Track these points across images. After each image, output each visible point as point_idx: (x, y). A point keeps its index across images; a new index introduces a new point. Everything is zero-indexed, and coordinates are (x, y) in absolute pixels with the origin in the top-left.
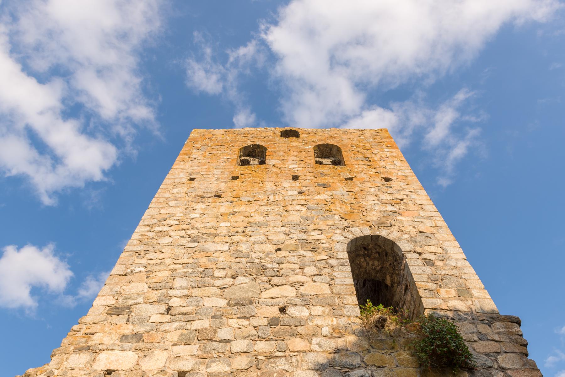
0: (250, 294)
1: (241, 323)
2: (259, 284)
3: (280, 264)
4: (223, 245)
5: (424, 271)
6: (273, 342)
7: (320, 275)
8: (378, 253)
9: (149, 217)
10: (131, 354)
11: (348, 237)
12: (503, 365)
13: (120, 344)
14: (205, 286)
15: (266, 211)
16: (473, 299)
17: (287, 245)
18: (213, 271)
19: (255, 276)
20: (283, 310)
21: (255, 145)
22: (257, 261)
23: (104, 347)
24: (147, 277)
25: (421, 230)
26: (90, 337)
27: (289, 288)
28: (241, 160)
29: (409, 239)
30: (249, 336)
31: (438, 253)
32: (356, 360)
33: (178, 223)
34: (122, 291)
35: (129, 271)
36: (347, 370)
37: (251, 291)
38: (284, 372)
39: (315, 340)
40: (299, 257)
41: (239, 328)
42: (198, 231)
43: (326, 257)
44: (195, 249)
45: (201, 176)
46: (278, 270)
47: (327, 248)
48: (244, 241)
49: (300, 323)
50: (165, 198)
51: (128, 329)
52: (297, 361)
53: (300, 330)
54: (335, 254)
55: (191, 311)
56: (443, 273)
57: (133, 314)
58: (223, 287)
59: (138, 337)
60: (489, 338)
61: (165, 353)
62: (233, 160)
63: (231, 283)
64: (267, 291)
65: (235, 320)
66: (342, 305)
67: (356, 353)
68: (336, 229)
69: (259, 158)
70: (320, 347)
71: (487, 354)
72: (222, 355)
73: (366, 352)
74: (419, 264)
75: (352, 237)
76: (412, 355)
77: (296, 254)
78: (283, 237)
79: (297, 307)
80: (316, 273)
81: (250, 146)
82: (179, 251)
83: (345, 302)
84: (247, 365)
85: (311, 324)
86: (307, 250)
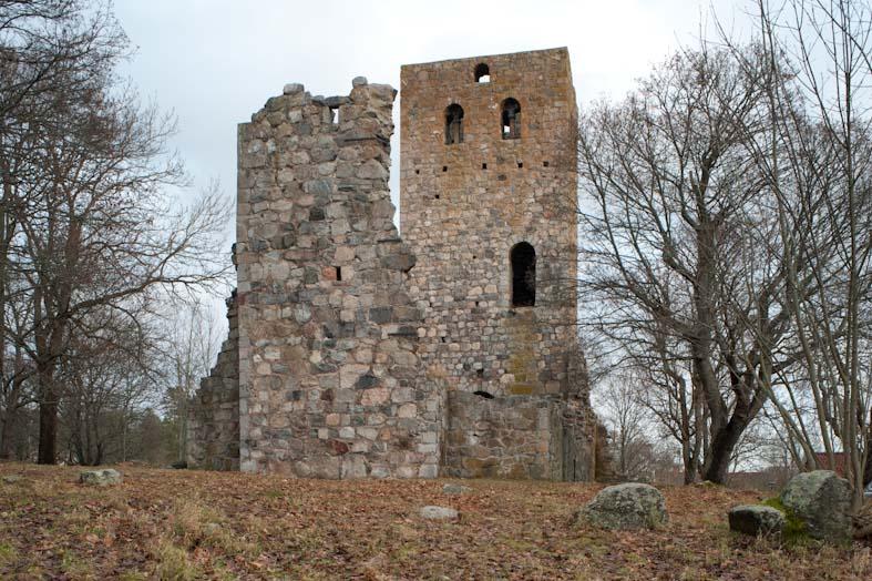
20: (477, 303)
32: (502, 331)
49: (484, 311)
53: (484, 315)
75: (512, 244)
78: (476, 245)
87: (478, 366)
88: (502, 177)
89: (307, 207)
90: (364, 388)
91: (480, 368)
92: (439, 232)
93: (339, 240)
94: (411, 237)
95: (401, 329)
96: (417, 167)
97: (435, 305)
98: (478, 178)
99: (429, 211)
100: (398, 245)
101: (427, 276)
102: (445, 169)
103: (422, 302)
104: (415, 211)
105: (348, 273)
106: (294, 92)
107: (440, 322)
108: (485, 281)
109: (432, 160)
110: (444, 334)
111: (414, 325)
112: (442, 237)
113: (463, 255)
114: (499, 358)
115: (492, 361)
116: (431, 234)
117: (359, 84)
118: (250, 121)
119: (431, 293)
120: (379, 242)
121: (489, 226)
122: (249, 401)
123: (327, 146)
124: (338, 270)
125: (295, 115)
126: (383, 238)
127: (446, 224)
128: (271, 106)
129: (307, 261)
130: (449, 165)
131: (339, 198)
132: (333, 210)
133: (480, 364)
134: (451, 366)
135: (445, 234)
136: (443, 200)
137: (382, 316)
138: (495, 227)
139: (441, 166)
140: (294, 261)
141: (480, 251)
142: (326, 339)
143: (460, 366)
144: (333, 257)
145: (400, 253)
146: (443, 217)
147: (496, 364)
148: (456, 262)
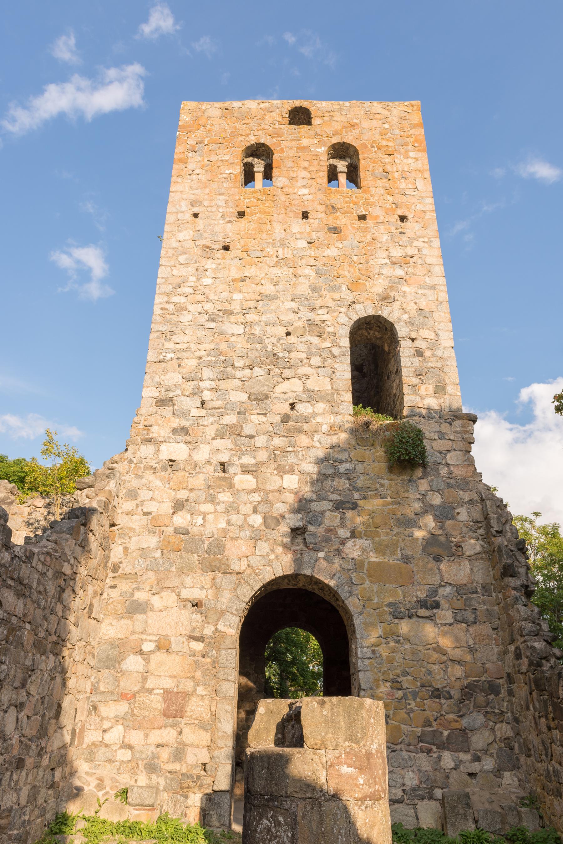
0: (266, 388)
1: (260, 420)
2: (273, 377)
3: (289, 352)
4: (238, 326)
5: (412, 364)
6: (285, 439)
7: (324, 367)
8: (379, 327)
9: (164, 280)
10: (182, 445)
11: (351, 317)
12: (449, 462)
13: (173, 437)
14: (228, 378)
15: (276, 275)
16: (445, 397)
17: (296, 328)
18: (233, 361)
19: (269, 367)
20: (292, 406)
21: (259, 143)
22: (270, 348)
23: (163, 440)
24: (179, 366)
25: (421, 308)
26: (149, 429)
27: (296, 380)
28: (244, 164)
29: (408, 320)
30: (267, 432)
31: (431, 340)
32: (345, 456)
33: (193, 292)
34: (162, 382)
35: (162, 357)
36: (338, 464)
37: (267, 385)
38: (293, 464)
39: (317, 437)
40: (306, 343)
41: (259, 424)
42: (213, 305)
43: (330, 345)
44: (214, 331)
45: (205, 208)
46: (288, 360)
47: (332, 333)
48: (257, 321)
49: (306, 420)
50: (173, 248)
51: (176, 423)
52: (303, 455)
53: (306, 427)
54: (338, 341)
55: (221, 406)
56: (429, 365)
57: (176, 407)
58: (243, 379)
59: (184, 431)
60: (446, 437)
61: (207, 446)
62: (236, 176)
63: (249, 375)
64: (280, 385)
65: (256, 416)
66: (339, 402)
67: (345, 450)
68: (341, 307)
69: (264, 158)
70: (320, 443)
71: (440, 453)
72: (249, 449)
73: (352, 449)
74: (411, 354)
75: (355, 318)
76: (385, 452)
77: (304, 340)
78: (292, 316)
79: (303, 403)
80: (320, 364)
81: (254, 144)
82: (201, 333)
83: (342, 399)
84: (267, 458)
85: (314, 421)
86: (313, 335)
88: (335, 230)
94: (176, 299)
96: (196, 210)
97: (208, 405)
99: (210, 265)
104: (186, 264)
107: (220, 435)
108: (306, 370)
110: (224, 457)
112: (230, 301)
113: (268, 328)
114: (339, 506)
115: (323, 512)
116: (212, 297)
119: (202, 385)
134: (237, 519)
135: (237, 296)
136: (235, 252)
138: (324, 293)
139: (235, 211)
141: (300, 324)
143: (257, 520)
146: (235, 273)
148: (253, 339)
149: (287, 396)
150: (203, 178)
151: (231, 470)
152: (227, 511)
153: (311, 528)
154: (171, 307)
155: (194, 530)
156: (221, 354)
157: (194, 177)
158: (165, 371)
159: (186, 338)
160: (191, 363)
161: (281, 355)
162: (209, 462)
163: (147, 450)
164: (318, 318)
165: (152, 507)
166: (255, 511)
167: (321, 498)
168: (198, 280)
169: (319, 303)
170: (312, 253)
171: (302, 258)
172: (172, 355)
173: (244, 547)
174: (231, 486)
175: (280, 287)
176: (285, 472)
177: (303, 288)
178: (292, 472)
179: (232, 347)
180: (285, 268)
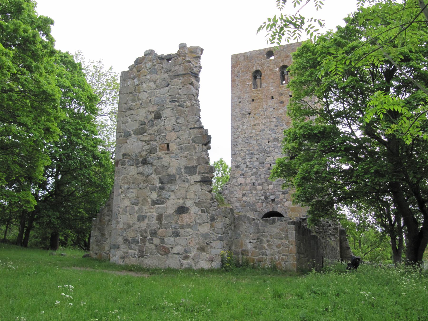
20: (271, 165)
51: (241, 172)
59: (243, 175)
78: (269, 136)
87: (272, 197)
88: (282, 102)
89: (153, 112)
90: (180, 214)
91: (273, 198)
92: (250, 131)
93: (169, 128)
94: (237, 134)
95: (202, 178)
96: (240, 100)
98: (270, 104)
99: (245, 121)
100: (201, 130)
101: (245, 152)
102: (253, 100)
103: (242, 165)
104: (238, 121)
105: (173, 147)
106: (150, 54)
107: (252, 175)
109: (246, 96)
110: (254, 181)
111: (209, 175)
112: (252, 133)
113: (263, 141)
115: (279, 195)
116: (247, 132)
117: (182, 46)
118: (128, 70)
119: (247, 160)
120: (191, 129)
121: (276, 126)
122: (117, 221)
123: (164, 79)
124: (168, 145)
125: (149, 65)
126: (192, 127)
127: (254, 126)
128: (138, 61)
129: (151, 141)
130: (255, 98)
131: (169, 106)
132: (166, 113)
133: (273, 196)
135: (254, 131)
136: (251, 115)
137: (191, 170)
138: (278, 127)
139: (251, 99)
140: (145, 141)
142: (160, 185)
143: (263, 198)
144: (165, 138)
145: (202, 134)
146: (253, 123)
147: (282, 196)
149: (269, 162)
150: (240, 87)
151: (256, 185)
152: (255, 196)
153: (276, 199)
154: (236, 136)
155: (248, 201)
156: (251, 150)
157: (238, 87)
158: (236, 157)
159: (241, 146)
160: (243, 154)
161: (267, 149)
162: (250, 183)
163: (234, 181)
164: (277, 136)
165: (237, 196)
166: (262, 196)
167: (279, 191)
168: (243, 126)
169: (277, 131)
170: (275, 112)
171: (272, 114)
172: (238, 152)
173: (260, 204)
174: (256, 189)
175: (266, 126)
176: (269, 184)
177: (273, 126)
178: (271, 184)
179: (253, 148)
180: (267, 119)
